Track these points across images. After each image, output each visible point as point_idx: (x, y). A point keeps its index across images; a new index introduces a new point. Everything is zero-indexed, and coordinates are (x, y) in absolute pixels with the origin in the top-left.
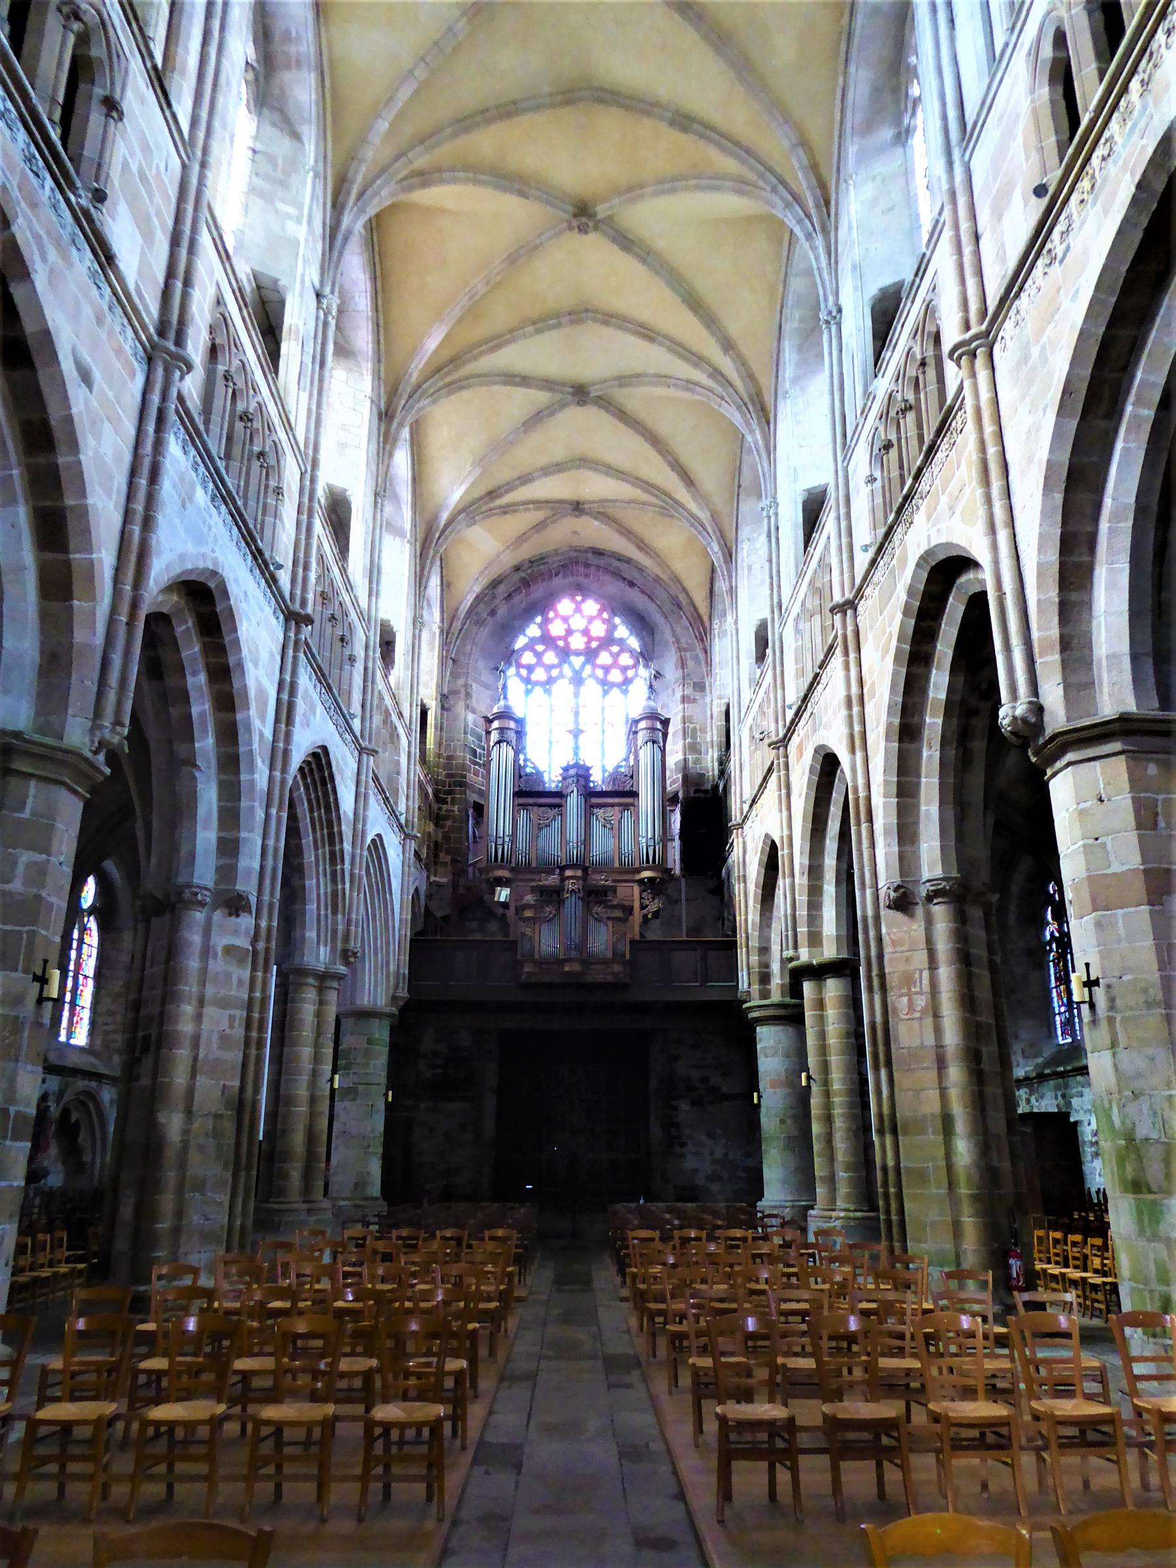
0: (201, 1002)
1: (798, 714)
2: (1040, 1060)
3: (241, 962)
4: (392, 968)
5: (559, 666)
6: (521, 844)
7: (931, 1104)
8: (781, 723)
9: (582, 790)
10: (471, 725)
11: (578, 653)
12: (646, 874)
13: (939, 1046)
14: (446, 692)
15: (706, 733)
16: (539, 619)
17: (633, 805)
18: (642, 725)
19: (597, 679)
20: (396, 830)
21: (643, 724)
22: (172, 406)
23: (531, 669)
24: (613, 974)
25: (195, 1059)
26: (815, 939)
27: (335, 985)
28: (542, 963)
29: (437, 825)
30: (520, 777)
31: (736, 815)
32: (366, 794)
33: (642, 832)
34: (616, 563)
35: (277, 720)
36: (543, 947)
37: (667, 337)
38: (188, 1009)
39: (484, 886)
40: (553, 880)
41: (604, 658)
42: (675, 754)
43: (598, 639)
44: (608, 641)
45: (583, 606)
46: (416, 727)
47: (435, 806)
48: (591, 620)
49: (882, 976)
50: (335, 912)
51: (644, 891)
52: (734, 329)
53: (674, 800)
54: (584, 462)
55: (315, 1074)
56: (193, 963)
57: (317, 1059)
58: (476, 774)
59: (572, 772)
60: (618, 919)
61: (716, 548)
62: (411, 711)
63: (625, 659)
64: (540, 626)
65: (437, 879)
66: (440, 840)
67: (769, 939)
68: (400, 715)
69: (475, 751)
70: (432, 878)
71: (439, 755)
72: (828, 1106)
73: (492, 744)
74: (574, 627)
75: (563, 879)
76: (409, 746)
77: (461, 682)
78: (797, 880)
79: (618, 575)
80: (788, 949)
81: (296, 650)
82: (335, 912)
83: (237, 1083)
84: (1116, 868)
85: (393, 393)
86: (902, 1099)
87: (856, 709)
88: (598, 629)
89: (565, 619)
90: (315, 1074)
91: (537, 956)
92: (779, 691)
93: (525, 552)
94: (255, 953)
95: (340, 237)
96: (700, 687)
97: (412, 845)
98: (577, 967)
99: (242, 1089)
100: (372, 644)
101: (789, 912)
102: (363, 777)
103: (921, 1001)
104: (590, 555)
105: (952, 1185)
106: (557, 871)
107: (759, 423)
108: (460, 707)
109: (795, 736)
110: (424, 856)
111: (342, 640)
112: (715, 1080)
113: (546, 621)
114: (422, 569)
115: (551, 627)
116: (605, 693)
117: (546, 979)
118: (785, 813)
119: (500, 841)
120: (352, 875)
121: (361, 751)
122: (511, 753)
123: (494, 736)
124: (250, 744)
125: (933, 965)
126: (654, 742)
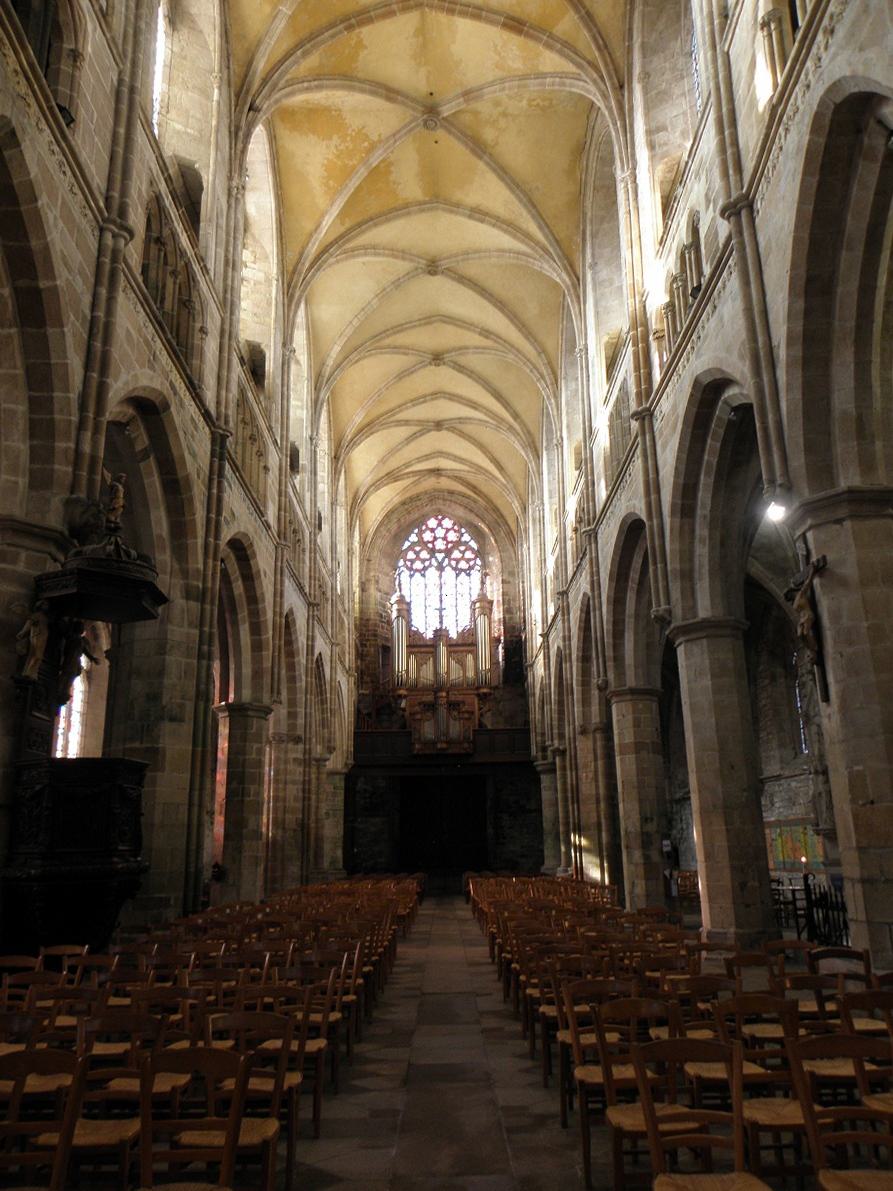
3: (300, 764)
4: (345, 748)
5: (430, 559)
7: (594, 820)
11: (440, 551)
13: (598, 794)
16: (416, 531)
18: (478, 605)
19: (451, 566)
21: (478, 605)
22: (285, 564)
23: (412, 561)
25: (285, 807)
26: (561, 736)
29: (362, 660)
31: (529, 662)
35: (307, 655)
37: (485, 408)
40: (429, 698)
41: (456, 554)
42: (498, 614)
43: (451, 542)
44: (458, 544)
48: (448, 530)
52: (520, 408)
53: (498, 640)
54: (441, 454)
55: (317, 808)
63: (469, 555)
65: (363, 691)
68: (345, 611)
70: (360, 692)
71: (361, 619)
74: (437, 536)
75: (436, 698)
77: (372, 574)
81: (313, 619)
82: (323, 728)
83: (301, 816)
84: (627, 741)
86: (584, 816)
87: (567, 643)
88: (452, 536)
89: (433, 530)
93: (408, 495)
95: (320, 402)
96: (512, 574)
97: (352, 680)
98: (444, 746)
99: (303, 820)
103: (591, 775)
104: (446, 494)
114: (352, 519)
115: (424, 535)
116: (457, 575)
117: (427, 752)
121: (332, 644)
124: (300, 670)
125: (596, 760)
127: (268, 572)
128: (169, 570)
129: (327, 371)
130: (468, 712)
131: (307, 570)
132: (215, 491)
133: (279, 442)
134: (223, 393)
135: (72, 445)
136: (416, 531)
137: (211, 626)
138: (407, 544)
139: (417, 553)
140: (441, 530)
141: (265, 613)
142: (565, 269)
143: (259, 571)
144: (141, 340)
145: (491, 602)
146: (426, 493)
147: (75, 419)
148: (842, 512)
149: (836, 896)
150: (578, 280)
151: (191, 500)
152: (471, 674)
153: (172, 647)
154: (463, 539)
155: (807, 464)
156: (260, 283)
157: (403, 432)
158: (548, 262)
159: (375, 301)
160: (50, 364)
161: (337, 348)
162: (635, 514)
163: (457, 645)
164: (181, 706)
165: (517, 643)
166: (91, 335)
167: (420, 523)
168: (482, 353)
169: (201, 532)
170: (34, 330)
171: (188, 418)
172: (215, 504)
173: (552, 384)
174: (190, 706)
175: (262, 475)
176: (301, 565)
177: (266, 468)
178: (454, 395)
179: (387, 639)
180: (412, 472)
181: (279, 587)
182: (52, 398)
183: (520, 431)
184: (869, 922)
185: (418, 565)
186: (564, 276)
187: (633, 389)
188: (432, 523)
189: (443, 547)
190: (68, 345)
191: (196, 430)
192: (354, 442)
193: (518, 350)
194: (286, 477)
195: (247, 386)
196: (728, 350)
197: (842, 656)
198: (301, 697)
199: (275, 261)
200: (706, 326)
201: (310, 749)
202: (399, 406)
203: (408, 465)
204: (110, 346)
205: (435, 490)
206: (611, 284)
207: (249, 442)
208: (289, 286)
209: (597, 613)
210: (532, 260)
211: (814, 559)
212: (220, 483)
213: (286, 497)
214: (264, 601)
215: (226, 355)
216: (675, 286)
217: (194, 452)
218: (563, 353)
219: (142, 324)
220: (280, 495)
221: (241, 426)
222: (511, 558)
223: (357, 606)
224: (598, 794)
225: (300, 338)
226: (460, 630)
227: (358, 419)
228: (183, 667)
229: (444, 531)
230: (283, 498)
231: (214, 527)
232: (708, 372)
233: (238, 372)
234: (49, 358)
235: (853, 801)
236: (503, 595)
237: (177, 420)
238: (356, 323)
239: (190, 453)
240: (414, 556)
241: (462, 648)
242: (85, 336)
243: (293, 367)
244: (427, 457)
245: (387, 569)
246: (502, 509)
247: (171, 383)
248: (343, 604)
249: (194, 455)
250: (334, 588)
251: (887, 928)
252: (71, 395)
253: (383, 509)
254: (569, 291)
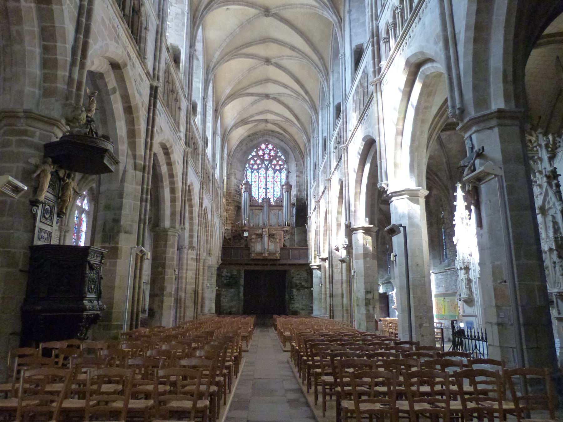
0: (187, 270)
2: (384, 279)
4: (217, 255)
5: (261, 164)
6: (251, 221)
7: (340, 291)
11: (266, 160)
13: (342, 280)
16: (255, 150)
18: (284, 187)
23: (253, 165)
25: (186, 282)
29: (227, 212)
34: (277, 135)
35: (199, 206)
37: (291, 88)
38: (184, 271)
39: (241, 232)
40: (260, 232)
41: (274, 162)
42: (294, 192)
43: (272, 156)
44: (276, 156)
45: (268, 146)
47: (226, 207)
48: (270, 150)
49: (332, 265)
52: (308, 88)
53: (294, 205)
55: (203, 283)
56: (185, 262)
57: (203, 280)
59: (265, 200)
61: (305, 138)
63: (280, 163)
64: (255, 152)
68: (219, 187)
70: (226, 228)
71: (227, 192)
72: (326, 291)
74: (266, 153)
75: (263, 232)
77: (233, 170)
79: (278, 138)
85: (217, 105)
88: (272, 153)
89: (263, 150)
90: (203, 283)
93: (252, 132)
94: (197, 259)
99: (195, 288)
103: (339, 270)
105: (343, 307)
107: (315, 114)
112: (303, 284)
113: (258, 151)
114: (223, 143)
116: (275, 173)
127: (180, 162)
128: (126, 154)
129: (212, 65)
131: (200, 164)
132: (151, 115)
133: (187, 97)
134: (157, 64)
135: (67, 74)
136: (255, 150)
137: (148, 185)
138: (250, 156)
139: (255, 161)
140: (266, 150)
141: (178, 183)
142: (335, 13)
143: (175, 161)
144: (111, 26)
146: (260, 131)
147: (69, 59)
148: (494, 122)
149: (468, 332)
150: (341, 19)
151: (138, 118)
152: (280, 220)
153: (127, 195)
154: (278, 155)
155: (474, 97)
156: (179, 14)
157: (250, 99)
158: (326, 10)
159: (237, 30)
160: (54, 27)
161: (218, 53)
162: (369, 135)
163: (273, 206)
164: (131, 226)
166: (80, 14)
167: (257, 146)
168: (291, 59)
169: (143, 135)
170: (45, 6)
171: (137, 73)
172: (151, 122)
173: (326, 75)
174: (136, 226)
175: (177, 112)
176: (197, 161)
177: (179, 108)
178: (276, 81)
180: (254, 120)
181: (185, 170)
182: (56, 46)
183: (308, 100)
184: (501, 347)
185: (255, 167)
186: (334, 17)
187: (370, 70)
188: (263, 146)
189: (268, 158)
190: (65, 16)
191: (142, 81)
192: (225, 103)
193: (309, 57)
194: (190, 115)
195: (171, 64)
196: (427, 41)
197: (490, 202)
198: (195, 228)
199: (187, 3)
200: (414, 30)
201: (200, 253)
202: (248, 86)
203: (252, 116)
204: (91, 22)
205: (265, 130)
206: (359, 21)
207: (171, 93)
208: (194, 17)
209: (347, 188)
210: (318, 9)
211: (476, 148)
212: (154, 111)
213: (190, 125)
214: (177, 176)
215: (159, 44)
216: (396, 12)
217: (140, 93)
218: (332, 59)
219: (112, 17)
220: (187, 123)
221: (166, 84)
222: (301, 165)
223: (225, 186)
224: (342, 280)
225: (199, 46)
226: (275, 199)
227: (228, 91)
228: (132, 205)
229: (268, 151)
230: (188, 125)
231: (150, 133)
232: (415, 55)
233: (165, 56)
234: (54, 23)
235: (494, 281)
237: (131, 73)
238: (227, 40)
239: (138, 93)
240: (254, 163)
241: (275, 208)
242: (76, 15)
243: (195, 62)
244: (261, 113)
245: (241, 169)
246: (297, 140)
247: (128, 53)
249: (140, 94)
250: (213, 175)
251: (511, 350)
252: (67, 46)
253: (239, 138)
254: (336, 25)
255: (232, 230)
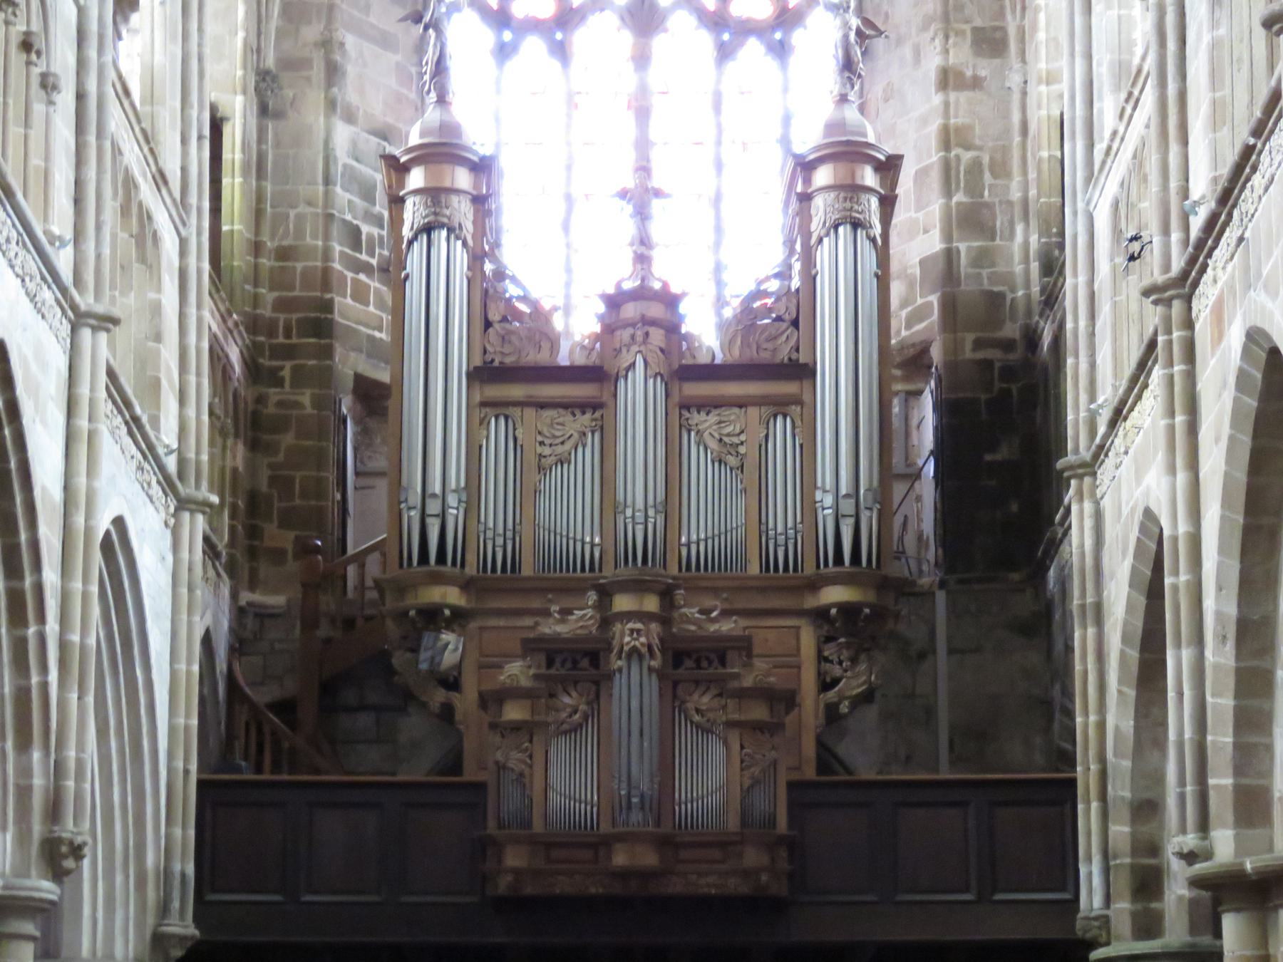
1: (1214, 227)
6: (493, 514)
8: (1175, 236)
9: (658, 363)
10: (342, 156)
12: (834, 595)
14: (270, 62)
15: (1008, 175)
17: (799, 402)
18: (823, 176)
20: (156, 491)
21: (823, 176)
24: (746, 874)
27: (29, 928)
28: (547, 845)
29: (254, 446)
30: (488, 324)
31: (1078, 444)
32: (92, 435)
33: (825, 475)
36: (555, 799)
46: (200, 199)
50: (24, 744)
51: (829, 639)
58: (360, 294)
60: (757, 727)
62: (185, 155)
65: (257, 597)
66: (264, 487)
67: (1158, 779)
68: (161, 179)
69: (356, 232)
70: (246, 597)
71: (257, 248)
73: (407, 232)
75: (606, 622)
76: (183, 253)
77: (311, 32)
78: (1208, 653)
80: (1183, 831)
91: (538, 826)
92: (1174, 149)
98: (648, 858)
100: (93, 27)
101: (1188, 734)
102: (84, 391)
106: (592, 597)
108: (312, 113)
109: (1207, 278)
110: (221, 546)
111: (26, 46)
116: (724, 53)
117: (563, 886)
118: (1182, 477)
119: (433, 507)
120: (63, 645)
121: (79, 319)
122: (461, 259)
123: (413, 213)
126: (856, 225)
130: (766, 694)
145: (889, 167)
163: (711, 372)
165: (1009, 373)
179: (374, 350)
236: (946, 145)
248: (148, 139)
255: (310, 623)
